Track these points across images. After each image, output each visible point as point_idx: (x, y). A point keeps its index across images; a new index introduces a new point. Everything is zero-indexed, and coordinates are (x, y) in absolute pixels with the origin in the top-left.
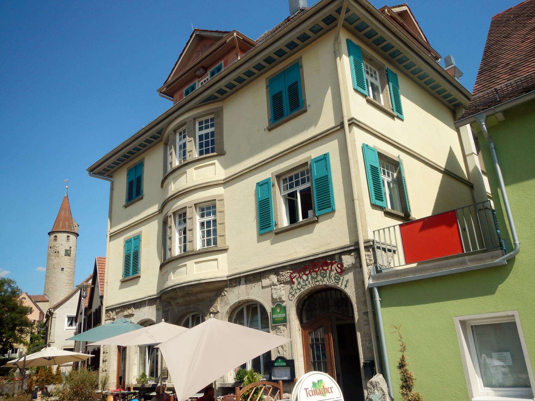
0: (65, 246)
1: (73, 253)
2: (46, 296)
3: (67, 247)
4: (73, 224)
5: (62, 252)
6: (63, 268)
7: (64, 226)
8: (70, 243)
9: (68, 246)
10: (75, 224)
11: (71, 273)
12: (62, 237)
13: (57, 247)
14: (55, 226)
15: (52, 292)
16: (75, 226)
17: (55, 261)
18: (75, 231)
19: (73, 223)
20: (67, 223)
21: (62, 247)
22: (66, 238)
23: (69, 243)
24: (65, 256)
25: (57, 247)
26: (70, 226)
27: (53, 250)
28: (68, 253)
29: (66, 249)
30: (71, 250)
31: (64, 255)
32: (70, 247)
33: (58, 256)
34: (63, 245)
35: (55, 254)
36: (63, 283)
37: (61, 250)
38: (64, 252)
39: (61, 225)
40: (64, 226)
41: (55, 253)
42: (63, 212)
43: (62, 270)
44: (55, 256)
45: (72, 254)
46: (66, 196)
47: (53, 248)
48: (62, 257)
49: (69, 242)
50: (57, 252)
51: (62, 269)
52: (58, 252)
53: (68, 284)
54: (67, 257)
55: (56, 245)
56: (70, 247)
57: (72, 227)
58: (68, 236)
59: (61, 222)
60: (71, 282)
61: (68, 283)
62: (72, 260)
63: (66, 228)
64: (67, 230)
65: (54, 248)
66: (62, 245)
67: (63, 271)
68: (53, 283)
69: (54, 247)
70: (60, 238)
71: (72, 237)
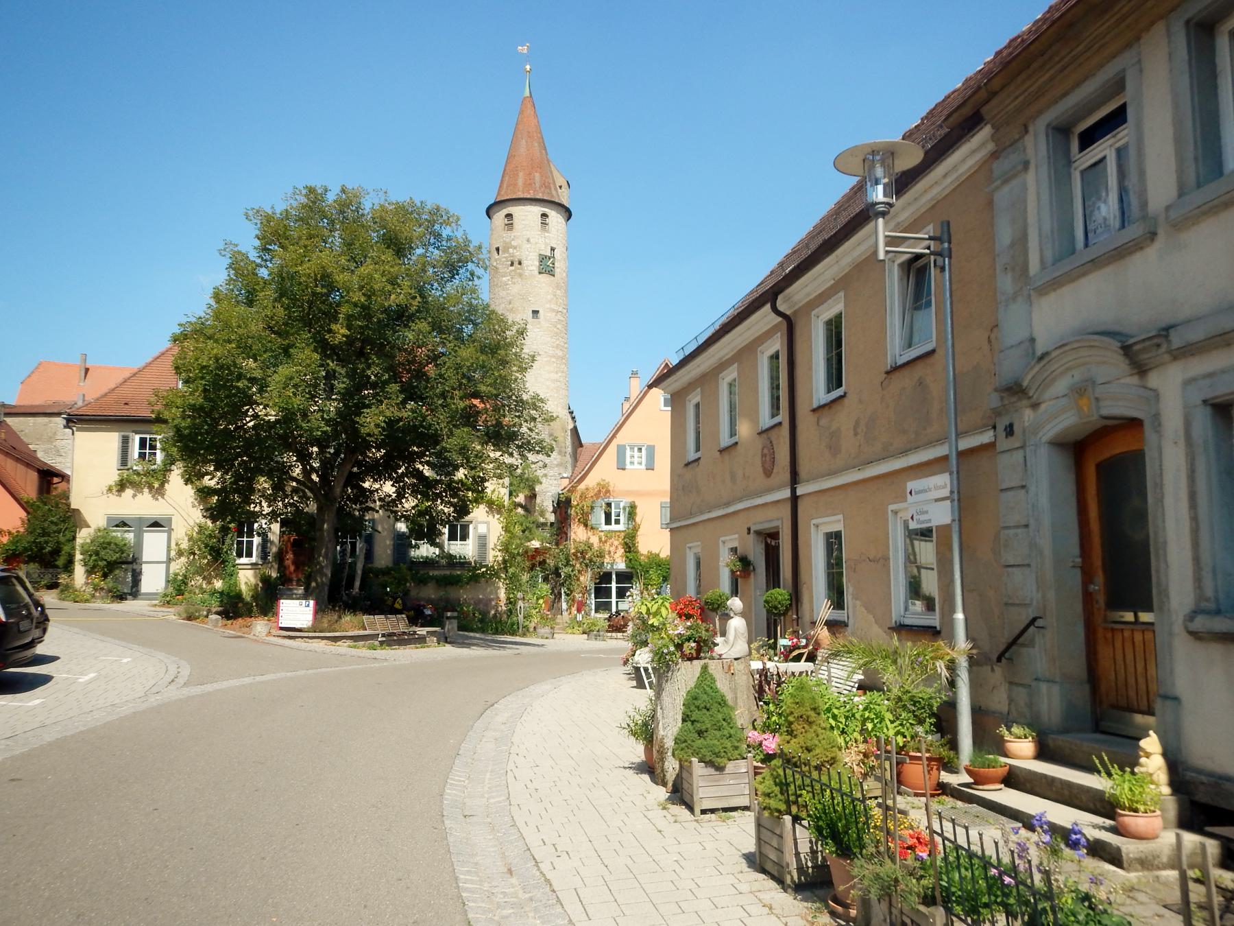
0: (536, 243)
1: (560, 267)
3: (543, 247)
4: (554, 181)
5: (532, 264)
6: (538, 312)
9: (546, 244)
10: (560, 181)
11: (559, 326)
12: (527, 215)
13: (515, 248)
14: (505, 186)
16: (560, 187)
17: (515, 289)
18: (559, 199)
19: (552, 176)
20: (537, 176)
21: (529, 246)
23: (547, 234)
24: (540, 273)
25: (515, 248)
26: (546, 186)
28: (546, 266)
29: (542, 253)
30: (554, 257)
31: (536, 272)
32: (553, 249)
33: (520, 275)
35: (512, 268)
37: (528, 255)
38: (537, 264)
39: (520, 182)
40: (530, 184)
41: (512, 264)
42: (523, 142)
43: (533, 318)
44: (513, 273)
45: (557, 271)
46: (527, 94)
47: (504, 252)
49: (548, 231)
50: (516, 264)
52: (520, 263)
53: (553, 360)
54: (545, 278)
56: (553, 249)
57: (553, 189)
59: (521, 174)
60: (560, 354)
61: (553, 356)
62: (558, 287)
64: (540, 196)
65: (506, 250)
66: (528, 240)
67: (537, 318)
70: (523, 220)
71: (555, 217)
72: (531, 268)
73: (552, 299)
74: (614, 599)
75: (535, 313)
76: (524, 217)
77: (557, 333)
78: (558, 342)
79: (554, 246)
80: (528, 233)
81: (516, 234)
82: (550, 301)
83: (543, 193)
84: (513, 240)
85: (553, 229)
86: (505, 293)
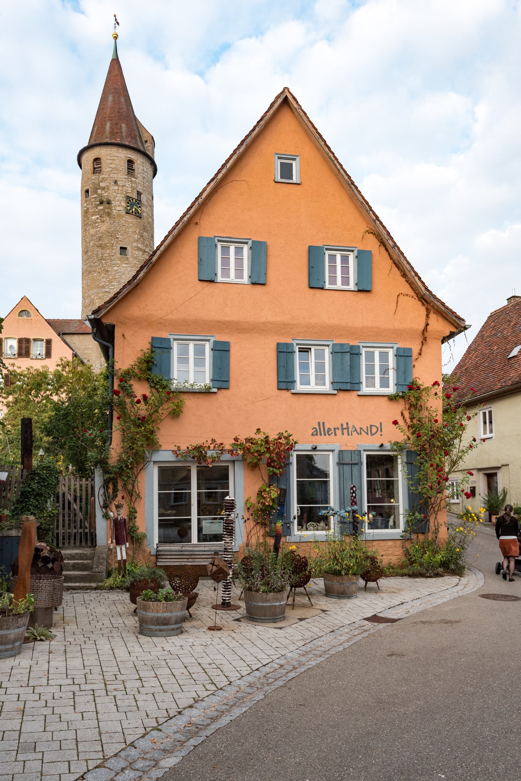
0: (123, 186)
6: (126, 248)
7: (113, 133)
8: (137, 180)
9: (133, 188)
20: (124, 125)
21: (116, 188)
22: (126, 167)
23: (133, 179)
25: (103, 189)
27: (94, 198)
31: (123, 213)
32: (139, 194)
33: (109, 214)
34: (119, 183)
35: (101, 207)
38: (124, 204)
40: (116, 133)
41: (101, 203)
48: (119, 216)
51: (123, 249)
52: (109, 203)
55: (102, 185)
56: (139, 194)
58: (130, 162)
59: (108, 125)
63: (121, 138)
65: (95, 192)
66: (116, 182)
68: (103, 287)
69: (96, 187)
70: (111, 164)
72: (118, 208)
73: (139, 239)
74: (194, 517)
75: (123, 249)
76: (111, 161)
79: (141, 191)
81: (103, 176)
82: (137, 241)
83: (130, 142)
85: (139, 176)
86: (94, 230)
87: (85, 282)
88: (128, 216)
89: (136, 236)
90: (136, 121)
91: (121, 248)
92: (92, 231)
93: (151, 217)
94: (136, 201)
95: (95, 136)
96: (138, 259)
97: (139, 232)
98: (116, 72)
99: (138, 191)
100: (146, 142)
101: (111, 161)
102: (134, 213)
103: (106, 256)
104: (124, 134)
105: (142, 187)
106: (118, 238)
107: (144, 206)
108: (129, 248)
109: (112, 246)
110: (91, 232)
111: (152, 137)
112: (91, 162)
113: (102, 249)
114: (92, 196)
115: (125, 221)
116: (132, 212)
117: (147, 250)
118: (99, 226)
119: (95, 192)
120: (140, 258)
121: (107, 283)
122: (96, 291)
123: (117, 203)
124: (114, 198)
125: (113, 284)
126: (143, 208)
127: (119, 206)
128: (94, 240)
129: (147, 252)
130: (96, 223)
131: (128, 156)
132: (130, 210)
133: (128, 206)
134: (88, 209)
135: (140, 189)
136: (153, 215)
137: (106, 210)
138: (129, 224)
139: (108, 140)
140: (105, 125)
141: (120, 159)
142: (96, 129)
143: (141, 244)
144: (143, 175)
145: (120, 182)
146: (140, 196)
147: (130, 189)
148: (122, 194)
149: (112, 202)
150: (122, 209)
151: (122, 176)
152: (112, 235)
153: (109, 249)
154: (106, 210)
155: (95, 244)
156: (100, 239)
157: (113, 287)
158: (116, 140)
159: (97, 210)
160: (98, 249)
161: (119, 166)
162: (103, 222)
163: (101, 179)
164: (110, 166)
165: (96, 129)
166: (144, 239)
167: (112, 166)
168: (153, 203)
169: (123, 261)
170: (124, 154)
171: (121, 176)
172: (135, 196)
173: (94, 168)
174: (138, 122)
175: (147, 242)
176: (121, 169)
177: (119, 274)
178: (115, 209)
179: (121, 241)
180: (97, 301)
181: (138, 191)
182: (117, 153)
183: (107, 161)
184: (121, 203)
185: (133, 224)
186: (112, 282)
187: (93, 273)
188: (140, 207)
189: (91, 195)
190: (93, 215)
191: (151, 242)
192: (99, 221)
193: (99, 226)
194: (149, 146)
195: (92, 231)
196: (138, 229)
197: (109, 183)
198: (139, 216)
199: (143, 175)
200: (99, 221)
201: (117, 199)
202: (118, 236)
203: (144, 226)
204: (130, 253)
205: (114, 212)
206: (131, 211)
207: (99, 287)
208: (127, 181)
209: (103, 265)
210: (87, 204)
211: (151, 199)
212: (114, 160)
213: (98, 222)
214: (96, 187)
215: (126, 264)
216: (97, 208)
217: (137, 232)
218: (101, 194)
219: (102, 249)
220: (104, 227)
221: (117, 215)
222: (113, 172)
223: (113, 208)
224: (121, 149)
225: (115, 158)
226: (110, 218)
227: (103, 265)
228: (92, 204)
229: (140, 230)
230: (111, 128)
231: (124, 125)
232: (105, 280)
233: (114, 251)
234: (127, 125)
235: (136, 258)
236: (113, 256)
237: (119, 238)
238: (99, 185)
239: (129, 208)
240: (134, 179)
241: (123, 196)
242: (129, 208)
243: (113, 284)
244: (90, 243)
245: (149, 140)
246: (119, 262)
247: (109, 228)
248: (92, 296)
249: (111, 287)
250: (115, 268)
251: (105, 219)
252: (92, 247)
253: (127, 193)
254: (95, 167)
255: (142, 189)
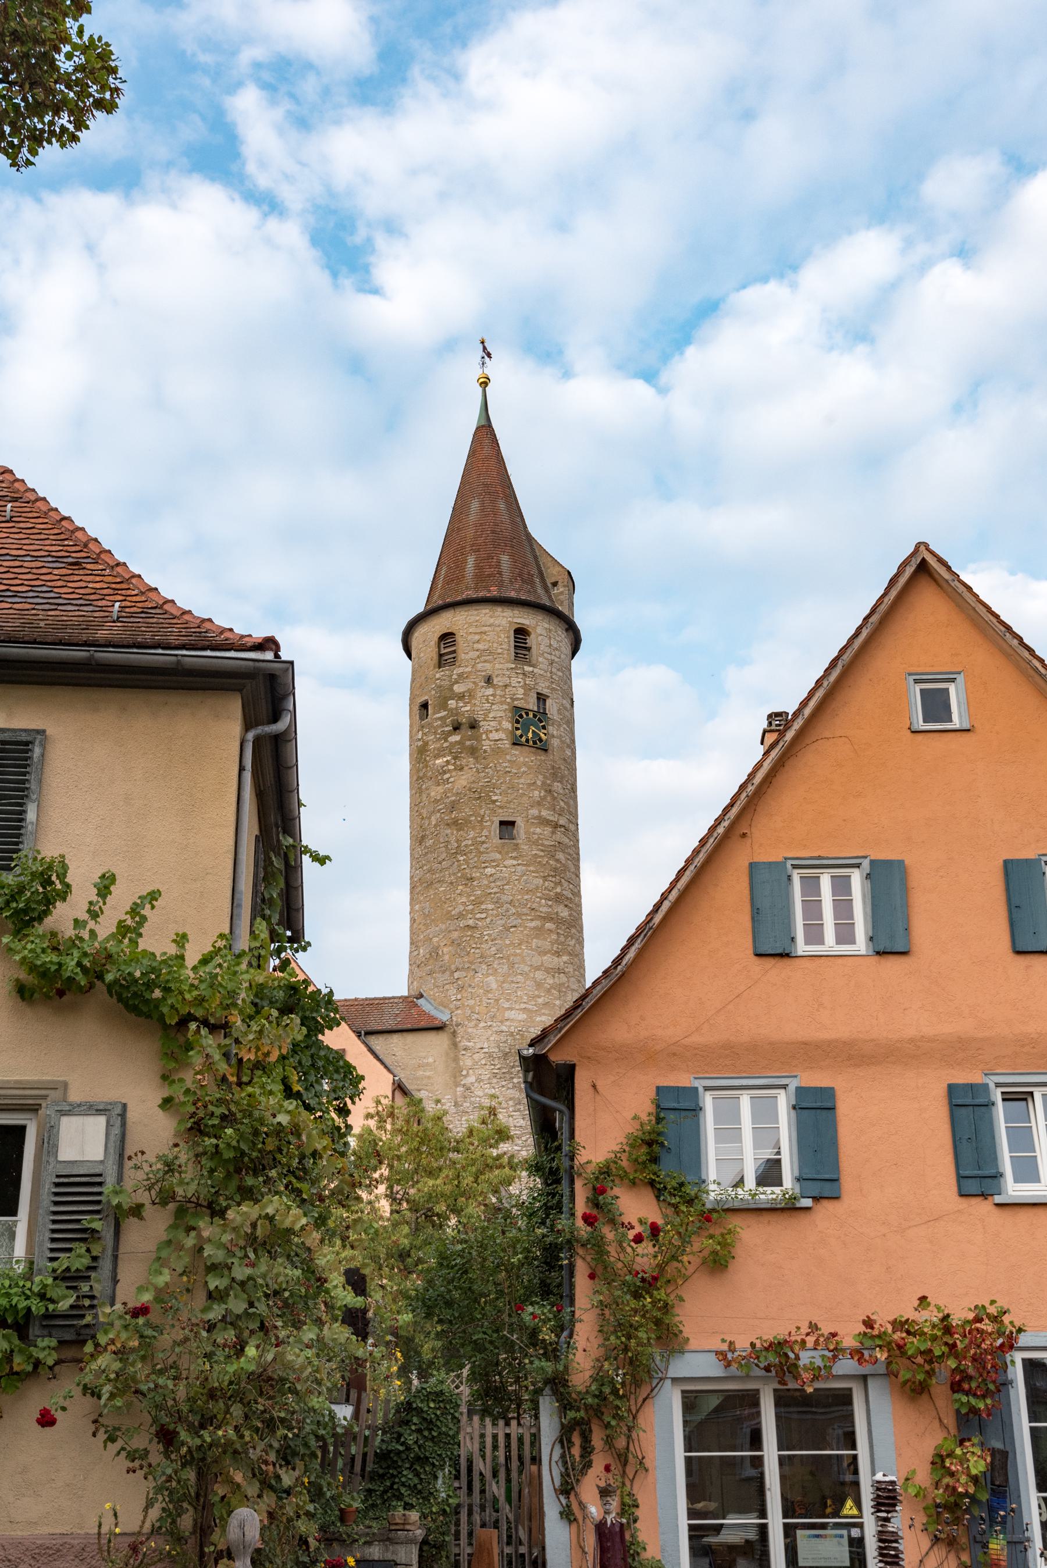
0: (506, 686)
2: (421, 1002)
6: (512, 824)
7: (480, 577)
8: (536, 670)
9: (527, 689)
15: (456, 975)
20: (505, 558)
21: (490, 691)
22: (512, 644)
23: (527, 669)
25: (461, 697)
27: (440, 719)
31: (507, 744)
32: (541, 698)
33: (473, 751)
35: (455, 738)
36: (519, 915)
38: (507, 725)
40: (489, 576)
41: (456, 728)
48: (498, 751)
52: (473, 726)
54: (524, 757)
55: (457, 688)
56: (541, 698)
58: (521, 633)
59: (471, 561)
61: (548, 918)
63: (501, 585)
65: (443, 706)
66: (489, 680)
68: (461, 916)
70: (478, 642)
72: (495, 736)
73: (543, 799)
75: (507, 825)
76: (477, 637)
77: (555, 869)
78: (558, 890)
79: (545, 691)
80: (488, 666)
81: (461, 670)
82: (539, 804)
84: (457, 682)
85: (541, 659)
86: (440, 789)
87: (417, 907)
88: (516, 751)
89: (536, 793)
90: (531, 546)
91: (502, 823)
92: (436, 792)
93: (569, 746)
94: (535, 716)
95: (443, 586)
96: (542, 845)
97: (544, 783)
98: (487, 450)
99: (538, 693)
100: (555, 584)
101: (477, 637)
102: (531, 743)
103: (466, 846)
104: (506, 575)
105: (547, 684)
106: (494, 802)
107: (553, 725)
108: (520, 822)
109: (482, 821)
110: (433, 794)
111: (569, 573)
112: (433, 643)
113: (458, 830)
114: (436, 715)
115: (509, 761)
116: (527, 741)
117: (561, 822)
118: (452, 780)
119: (443, 706)
120: (546, 843)
121: (471, 907)
122: (443, 927)
123: (492, 723)
124: (486, 715)
125: (483, 907)
126: (550, 728)
127: (497, 730)
128: (439, 811)
129: (561, 826)
130: (445, 772)
131: (515, 620)
132: (521, 736)
133: (517, 729)
134: (426, 744)
135: (543, 688)
136: (573, 741)
137: (468, 743)
138: (520, 768)
139: (471, 594)
140: (465, 561)
141: (498, 629)
142: (443, 572)
143: (548, 809)
144: (549, 657)
145: (499, 679)
146: (545, 704)
147: (521, 691)
148: (502, 703)
149: (481, 723)
150: (503, 736)
151: (502, 666)
152: (481, 795)
153: (473, 828)
154: (468, 743)
155: (442, 819)
156: (453, 807)
157: (483, 916)
158: (489, 591)
159: (445, 745)
160: (449, 831)
161: (495, 645)
162: (461, 769)
163: (455, 677)
164: (476, 646)
165: (443, 572)
166: (554, 799)
167: (480, 646)
168: (572, 715)
169: (507, 853)
170: (506, 618)
171: (501, 666)
172: (532, 704)
173: (441, 655)
174: (535, 547)
175: (562, 804)
176: (500, 651)
177: (498, 883)
178: (488, 738)
179: (500, 807)
180: (445, 950)
181: (538, 693)
182: (491, 617)
183: (469, 638)
184: (500, 723)
185: (529, 768)
186: (482, 903)
187: (438, 885)
188: (544, 727)
189: (434, 713)
190: (437, 757)
191: (572, 802)
192: (451, 767)
193: (452, 780)
194: (562, 593)
195: (436, 792)
196: (541, 777)
197: (474, 683)
198: (541, 746)
199: (549, 657)
200: (451, 767)
201: (491, 715)
202: (494, 798)
203: (553, 767)
204: (522, 832)
205: (486, 745)
206: (524, 739)
207: (452, 918)
208: (513, 675)
209: (459, 866)
210: (424, 734)
211: (568, 706)
212: (485, 633)
213: (449, 771)
214: (445, 696)
215: (514, 858)
216: (446, 740)
217: (539, 783)
218: (456, 708)
219: (458, 830)
220: (462, 781)
221: (493, 750)
222: (483, 658)
223: (484, 737)
224: (499, 609)
225: (486, 629)
226: (476, 758)
227: (459, 866)
228: (435, 733)
229: (545, 777)
230: (478, 567)
231: (505, 558)
232: (464, 899)
233: (485, 833)
234: (511, 555)
235: (536, 843)
236: (483, 843)
237: (496, 801)
238: (451, 690)
239: (519, 733)
240: (531, 669)
241: (505, 707)
242: (519, 733)
243: (483, 907)
244: (430, 818)
245: (563, 579)
246: (498, 856)
247: (474, 782)
248: (435, 940)
249: (478, 916)
250: (489, 871)
251: (464, 762)
252: (436, 826)
253: (513, 700)
254: (443, 651)
255: (548, 688)
